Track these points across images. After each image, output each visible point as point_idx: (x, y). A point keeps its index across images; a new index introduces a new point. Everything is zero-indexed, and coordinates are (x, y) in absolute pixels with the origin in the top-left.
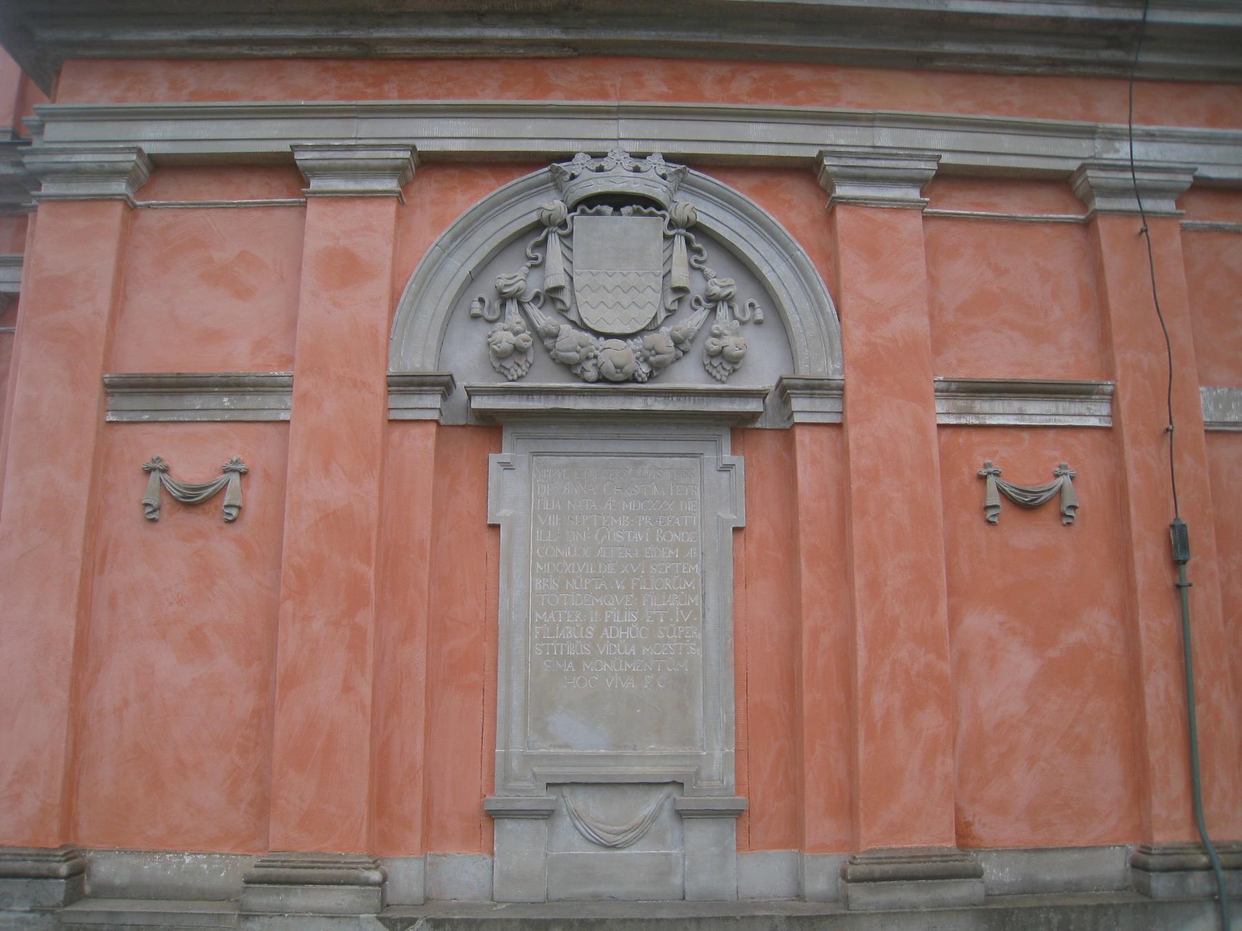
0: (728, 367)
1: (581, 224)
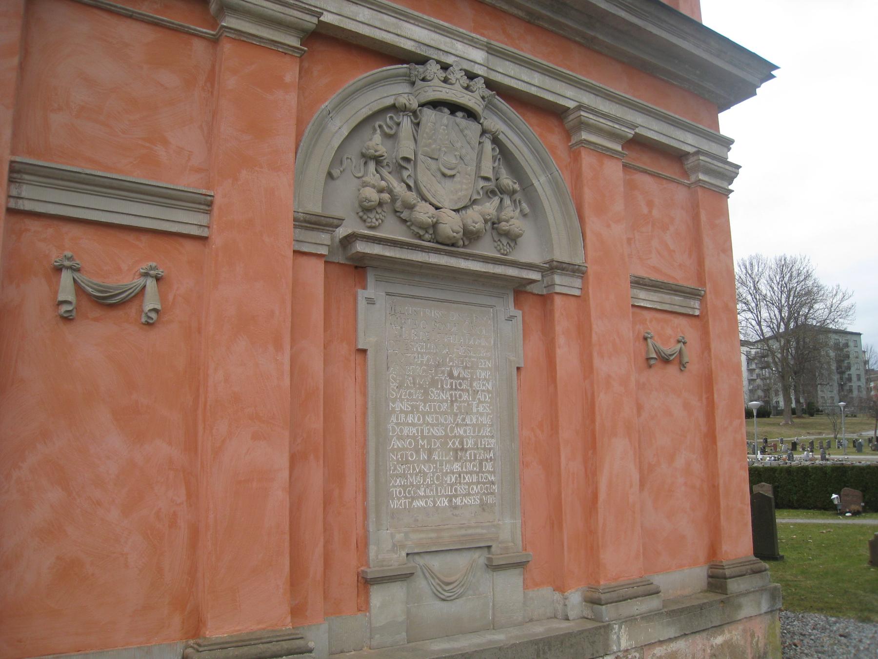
0: (512, 245)
1: (429, 116)
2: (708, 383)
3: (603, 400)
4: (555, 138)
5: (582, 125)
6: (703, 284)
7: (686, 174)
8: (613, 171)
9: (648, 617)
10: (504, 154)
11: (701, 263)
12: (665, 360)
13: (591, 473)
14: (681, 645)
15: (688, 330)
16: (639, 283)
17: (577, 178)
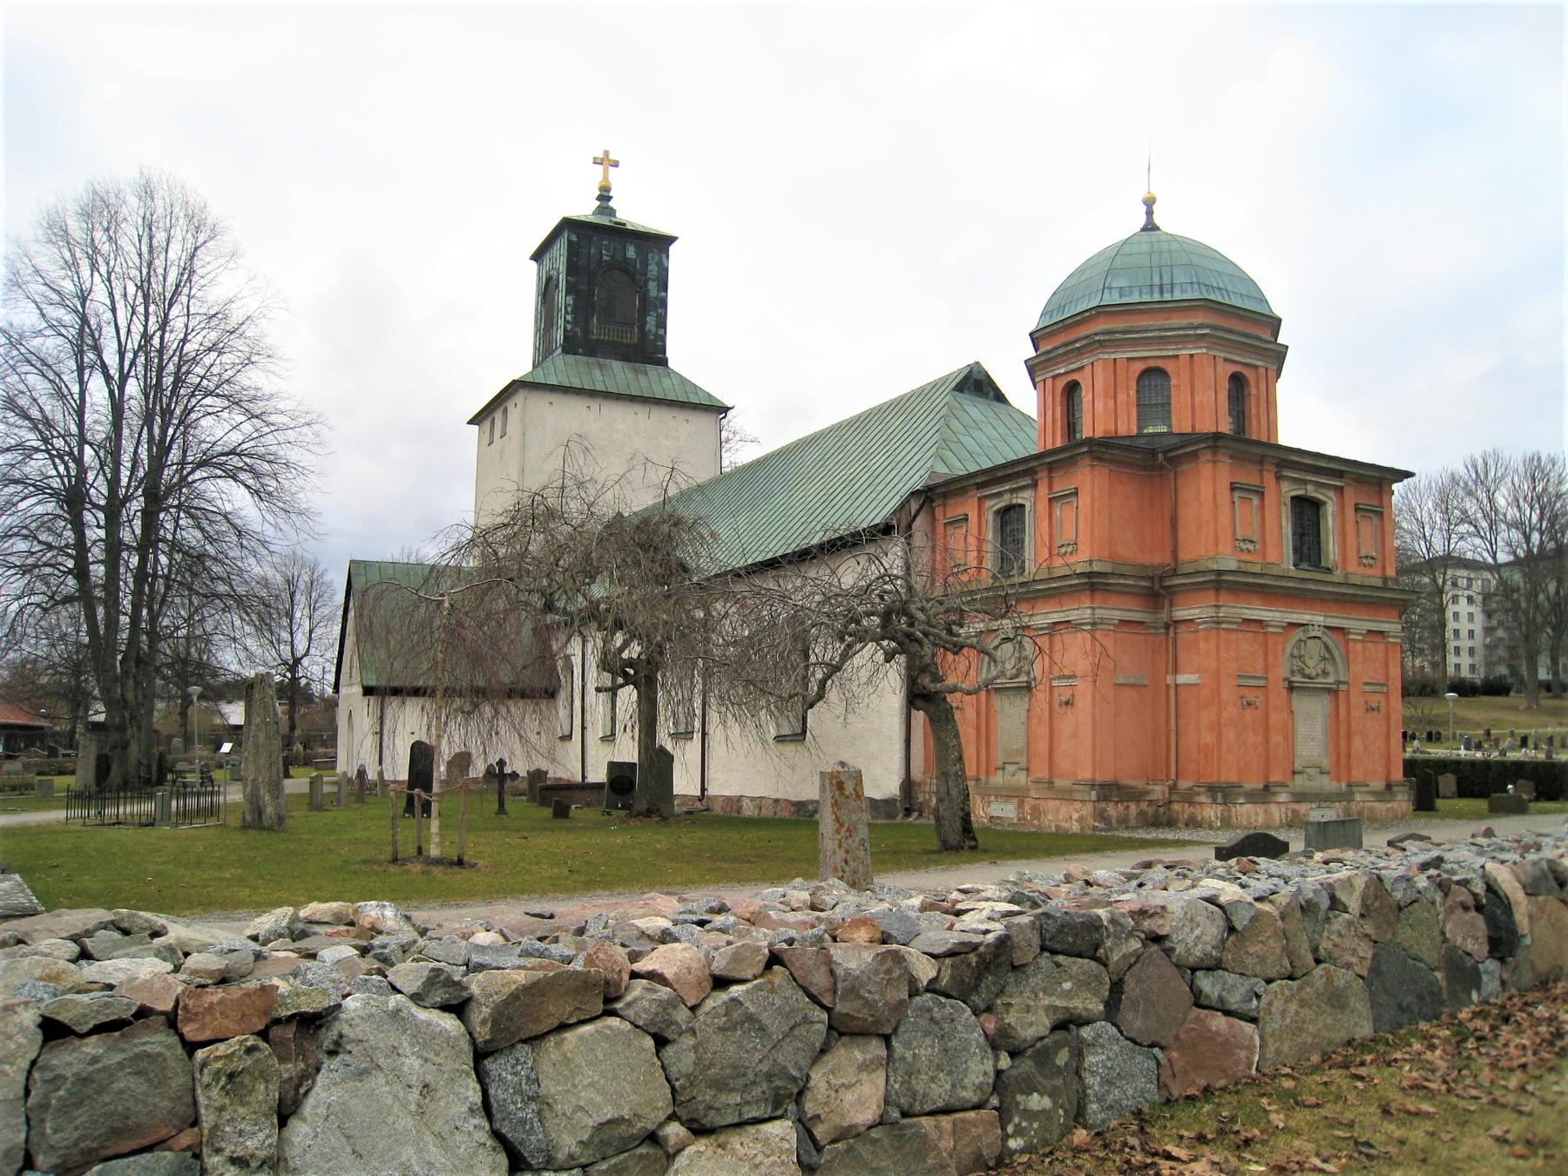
2: (1388, 717)
3: (1353, 724)
4: (1341, 637)
5: (1350, 633)
6: (1387, 679)
7: (1384, 638)
8: (1359, 646)
9: (1366, 792)
10: (1326, 647)
11: (1387, 672)
12: (1373, 710)
13: (1349, 747)
14: (1376, 804)
15: (1380, 697)
16: (1366, 684)
17: (1347, 651)
